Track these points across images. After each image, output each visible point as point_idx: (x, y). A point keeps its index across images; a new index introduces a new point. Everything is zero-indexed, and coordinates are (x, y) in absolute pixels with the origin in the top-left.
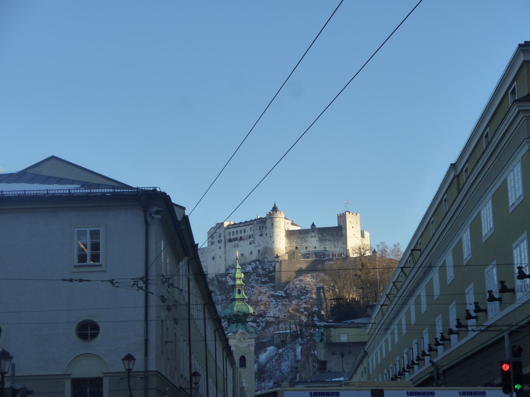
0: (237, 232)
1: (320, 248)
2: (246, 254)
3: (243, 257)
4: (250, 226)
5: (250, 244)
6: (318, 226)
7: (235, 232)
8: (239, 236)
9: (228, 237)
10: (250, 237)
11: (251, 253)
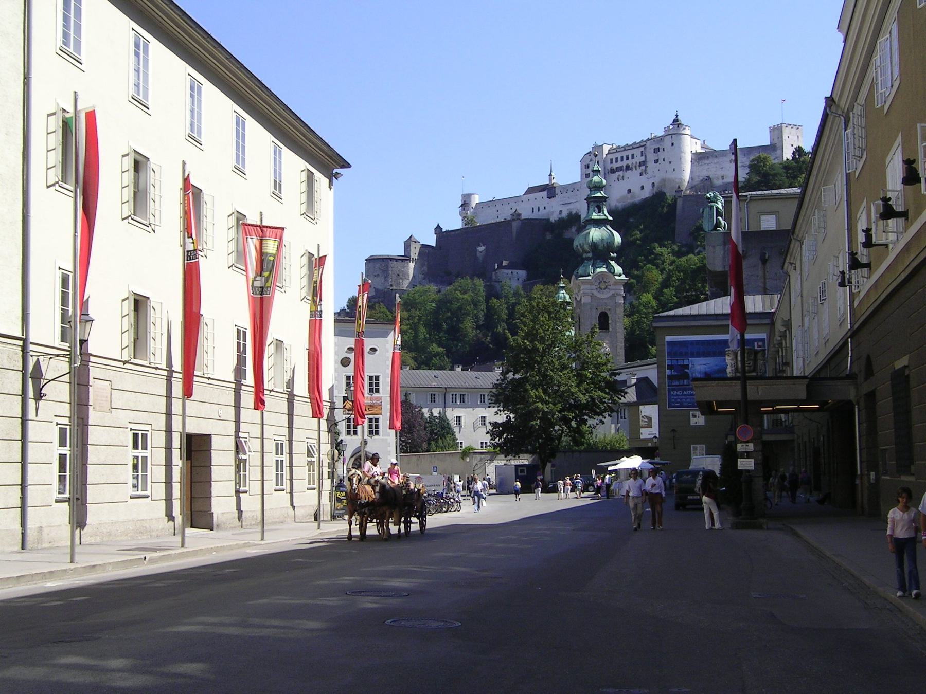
0: (622, 158)
2: (636, 189)
3: (630, 194)
4: (642, 149)
7: (619, 159)
9: (609, 166)
11: (642, 187)
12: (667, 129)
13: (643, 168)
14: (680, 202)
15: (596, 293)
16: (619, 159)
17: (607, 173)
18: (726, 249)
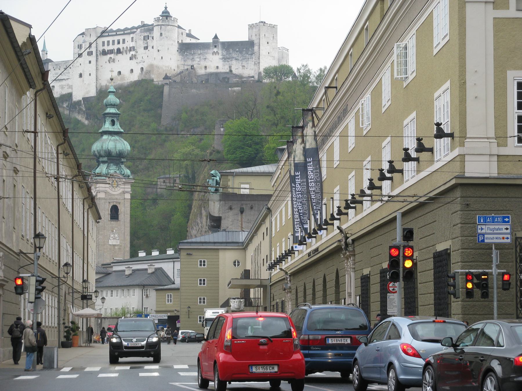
1: (223, 68)
2: (126, 72)
3: (120, 76)
4: (132, 35)
5: (131, 59)
6: (222, 39)
7: (111, 43)
8: (116, 47)
9: (101, 48)
10: (130, 50)
11: (132, 71)
12: (158, 20)
13: (133, 53)
14: (166, 89)
15: (109, 190)
16: (111, 43)
17: (99, 54)
18: (221, 204)
